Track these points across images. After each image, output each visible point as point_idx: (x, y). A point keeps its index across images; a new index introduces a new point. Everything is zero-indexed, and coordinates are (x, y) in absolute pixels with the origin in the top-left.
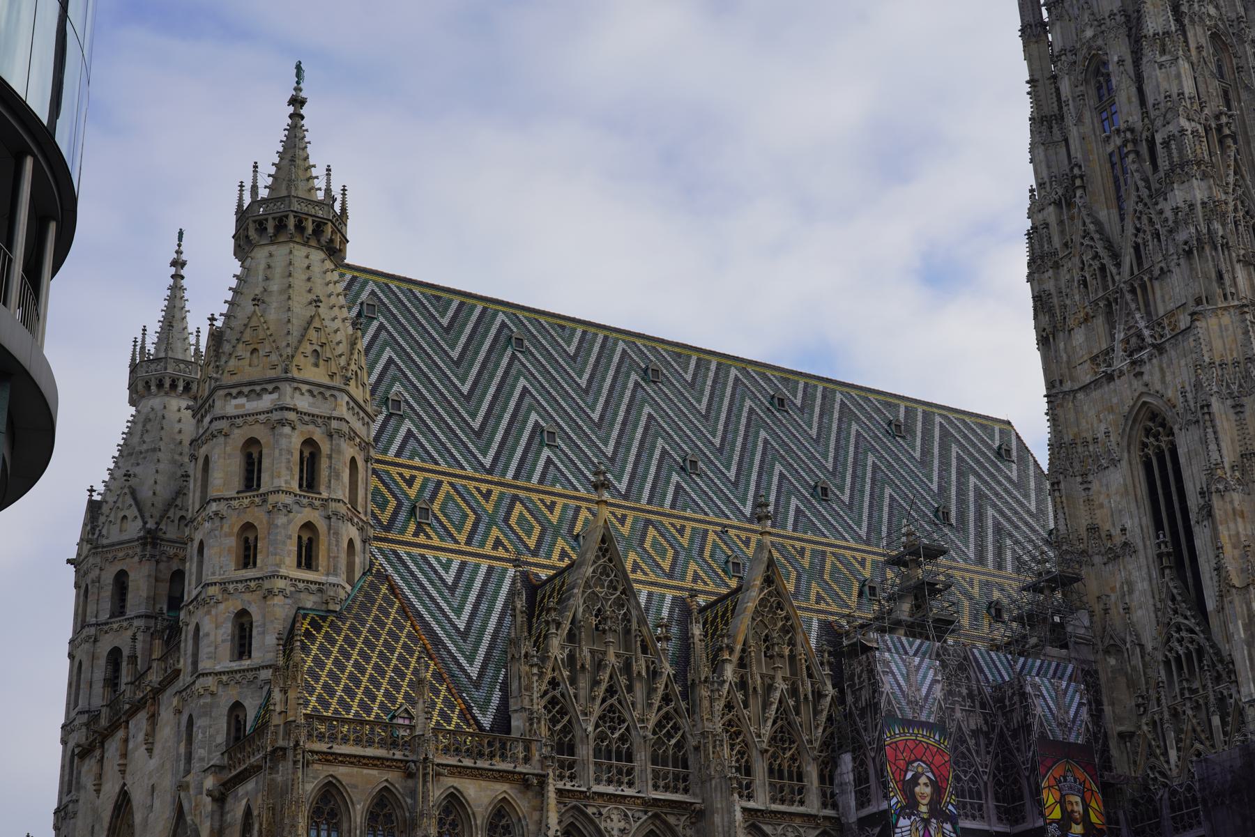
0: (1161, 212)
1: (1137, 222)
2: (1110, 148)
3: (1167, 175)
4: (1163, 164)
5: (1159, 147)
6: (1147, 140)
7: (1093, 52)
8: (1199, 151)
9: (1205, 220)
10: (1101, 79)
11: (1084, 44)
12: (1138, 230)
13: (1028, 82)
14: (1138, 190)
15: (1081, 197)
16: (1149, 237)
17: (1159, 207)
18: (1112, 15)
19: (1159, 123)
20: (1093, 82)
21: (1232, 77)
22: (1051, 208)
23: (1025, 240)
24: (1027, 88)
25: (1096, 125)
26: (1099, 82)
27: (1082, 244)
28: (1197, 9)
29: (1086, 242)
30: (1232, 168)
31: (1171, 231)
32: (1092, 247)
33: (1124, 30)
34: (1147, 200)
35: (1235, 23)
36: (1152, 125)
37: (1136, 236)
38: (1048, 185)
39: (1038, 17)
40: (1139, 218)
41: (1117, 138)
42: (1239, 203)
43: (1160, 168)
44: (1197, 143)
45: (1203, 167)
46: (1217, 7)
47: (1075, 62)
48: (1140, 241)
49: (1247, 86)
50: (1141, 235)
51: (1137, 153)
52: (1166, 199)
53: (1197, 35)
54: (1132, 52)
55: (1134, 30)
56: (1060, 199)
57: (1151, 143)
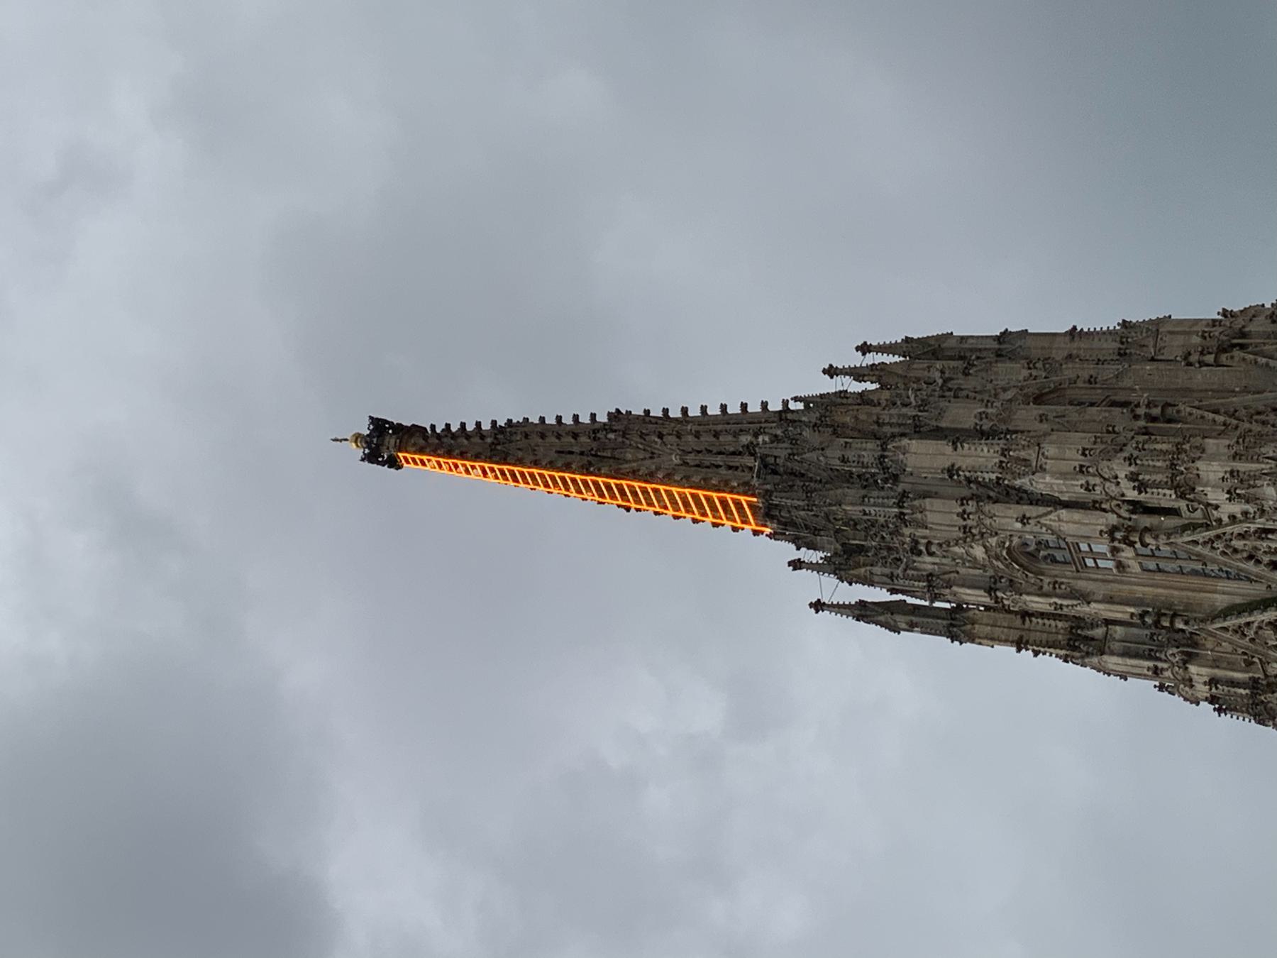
0: (1233, 518)
1: (1239, 556)
2: (1135, 567)
3: (1182, 496)
4: (1166, 498)
5: (1142, 497)
6: (1132, 512)
7: (1004, 553)
8: (1164, 447)
9: (1258, 461)
10: (1042, 553)
11: (991, 563)
12: (1251, 557)
13: (1019, 650)
14: (1195, 542)
15: (1186, 623)
16: (1265, 545)
17: (1225, 519)
18: (962, 515)
19: (1112, 489)
20: (1044, 566)
21: (1099, 391)
22: (1193, 669)
23: (1226, 718)
24: (1027, 654)
25: (1100, 577)
26: (1045, 558)
27: (1252, 640)
28: (994, 411)
29: (1251, 633)
30: (1206, 414)
31: (1263, 512)
32: (1260, 628)
33: (988, 507)
34: (1212, 533)
35: (1034, 373)
36: (1113, 498)
37: (1258, 562)
38: (1160, 665)
39: (943, 614)
40: (1236, 551)
41: (1123, 554)
42: (1255, 417)
43: (1176, 505)
44: (1152, 446)
45: (1187, 447)
46: (1005, 390)
47: (1011, 581)
48: (1266, 559)
49: (1117, 377)
50: (1259, 555)
51: (1146, 530)
52: (1217, 507)
53: (1026, 416)
54: (1018, 503)
55: (992, 494)
56: (1183, 653)
57: (1137, 507)
